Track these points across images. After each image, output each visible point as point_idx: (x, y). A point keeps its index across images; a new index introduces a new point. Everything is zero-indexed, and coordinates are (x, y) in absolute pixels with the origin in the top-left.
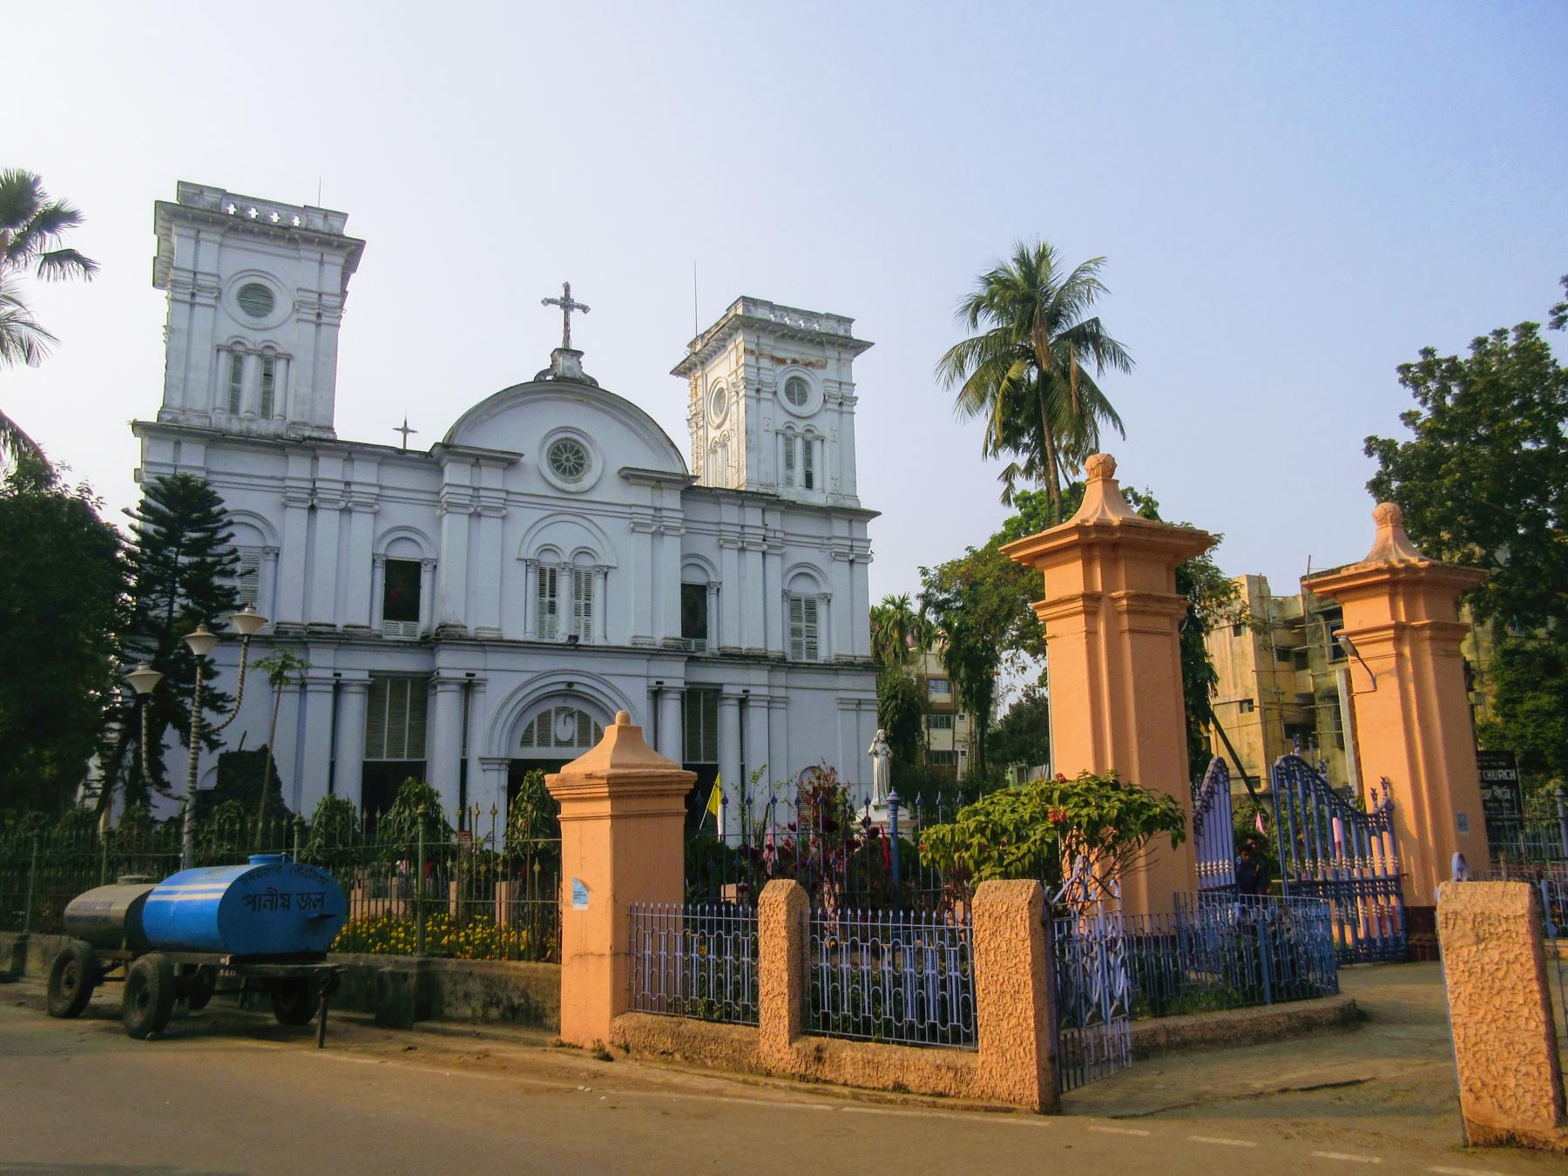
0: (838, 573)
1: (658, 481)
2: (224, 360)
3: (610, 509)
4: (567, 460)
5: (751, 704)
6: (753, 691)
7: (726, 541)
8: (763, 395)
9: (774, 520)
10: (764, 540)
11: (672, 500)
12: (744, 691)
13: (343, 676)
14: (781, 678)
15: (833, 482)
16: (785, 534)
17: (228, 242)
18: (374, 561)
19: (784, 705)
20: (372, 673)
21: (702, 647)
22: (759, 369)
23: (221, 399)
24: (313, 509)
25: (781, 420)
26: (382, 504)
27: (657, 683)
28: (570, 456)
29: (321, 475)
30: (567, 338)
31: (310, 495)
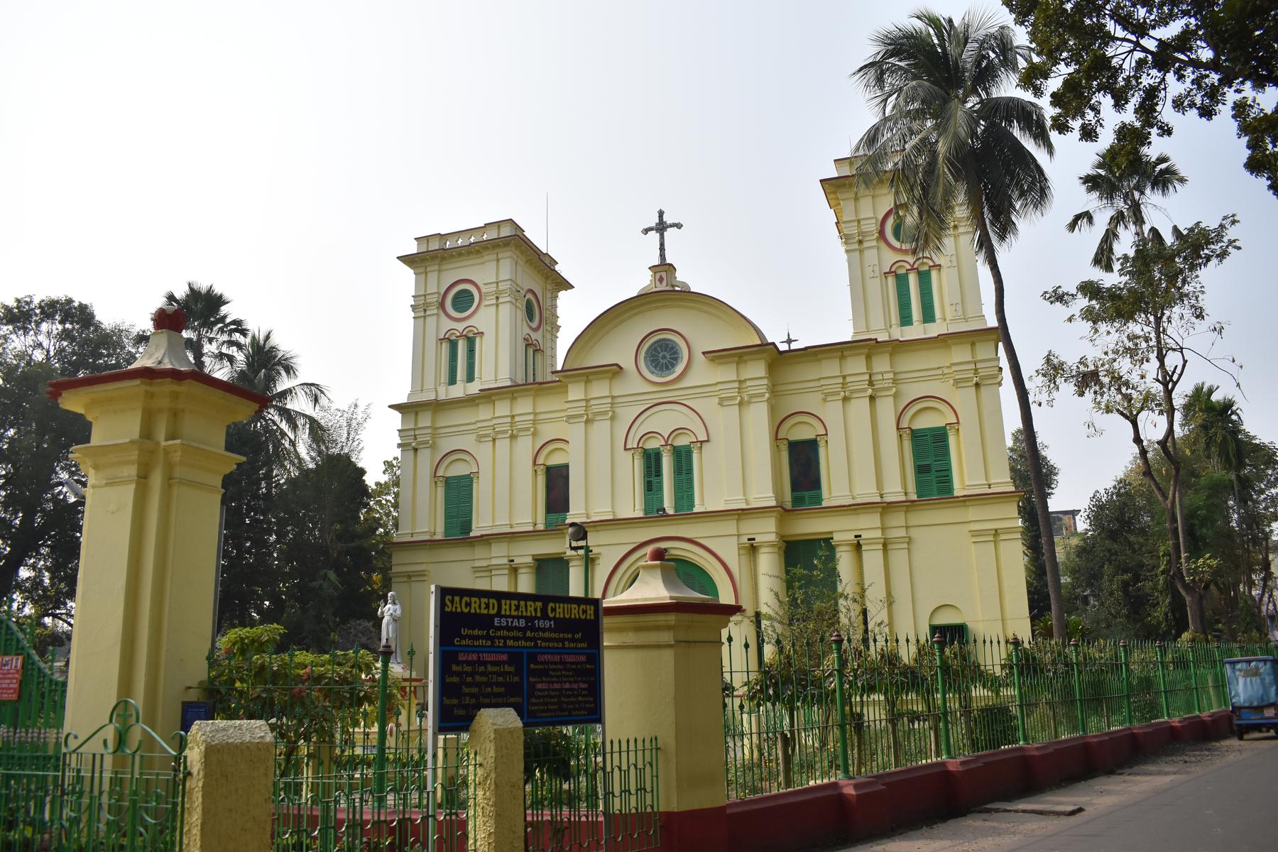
0: (963, 399)
1: (738, 355)
2: (445, 347)
3: (703, 390)
4: (664, 357)
6: (865, 535)
7: (827, 395)
8: (866, 245)
9: (882, 364)
10: (871, 383)
11: (756, 370)
12: (856, 536)
14: (897, 519)
15: (954, 308)
17: (444, 267)
18: (536, 471)
21: (818, 499)
22: (859, 221)
23: (444, 376)
24: (494, 440)
27: (749, 540)
28: (666, 353)
30: (662, 256)
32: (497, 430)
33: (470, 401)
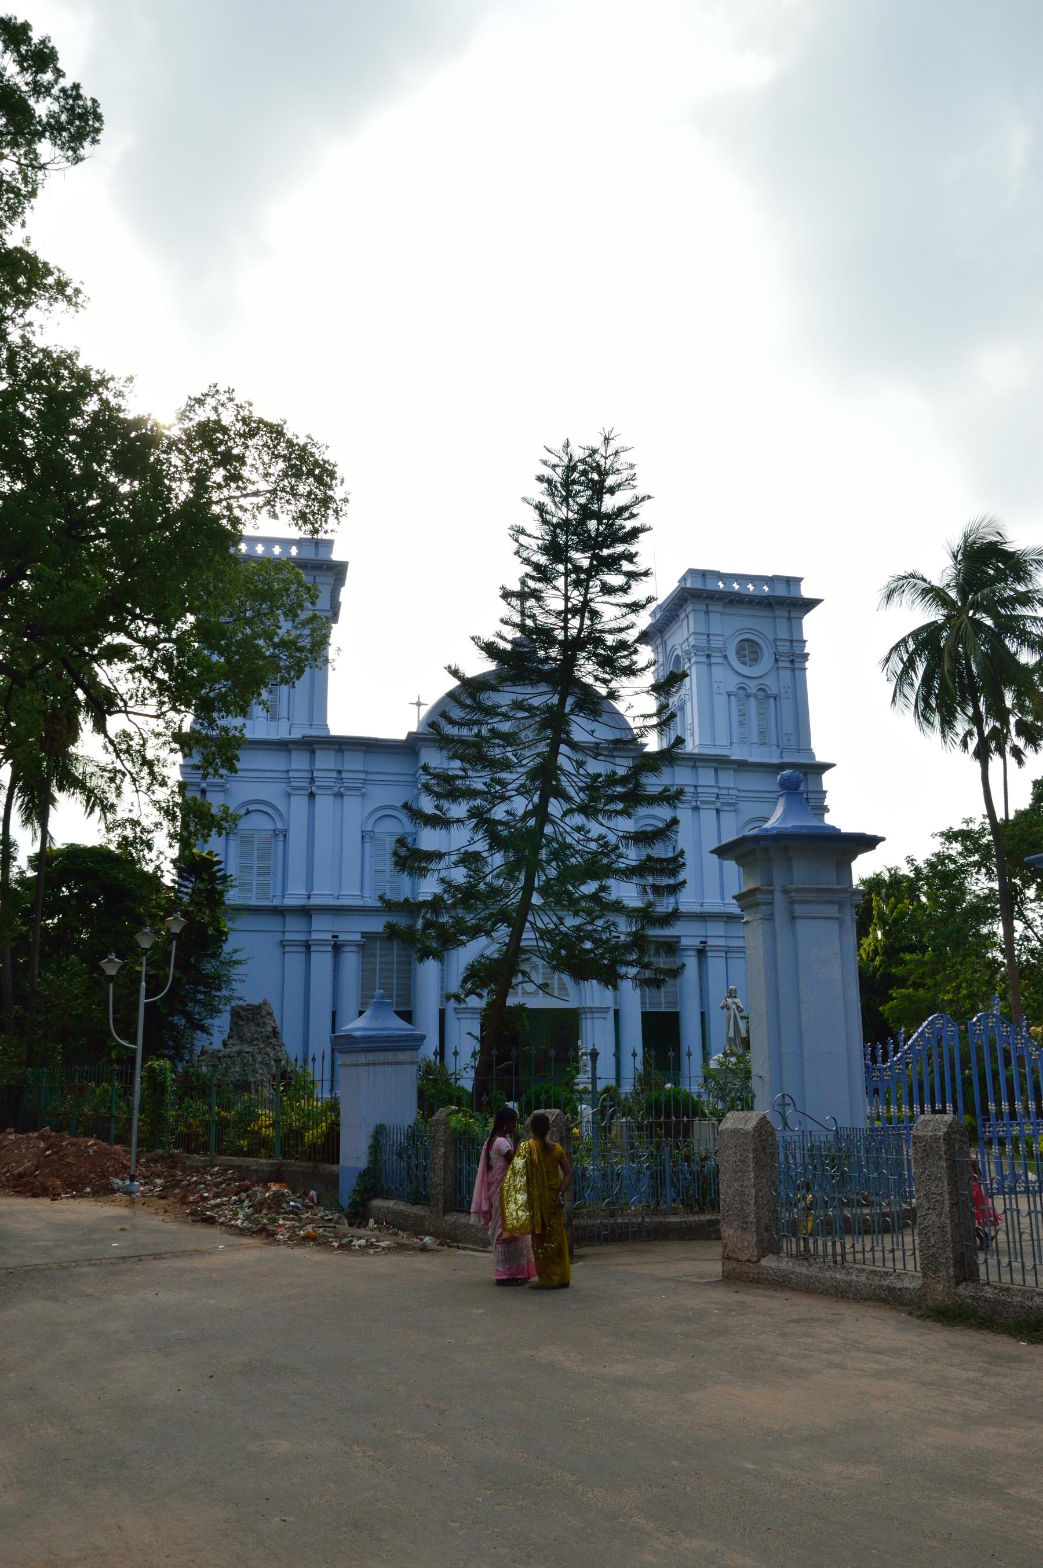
5: (709, 954)
6: (711, 942)
8: (713, 660)
9: (728, 779)
10: (718, 798)
12: (702, 942)
13: (340, 938)
16: (739, 791)
18: (363, 837)
19: (742, 955)
20: (364, 934)
22: (708, 635)
24: (312, 795)
25: (732, 683)
26: (368, 787)
29: (317, 767)
31: (310, 783)
32: (317, 784)
33: (284, 746)
